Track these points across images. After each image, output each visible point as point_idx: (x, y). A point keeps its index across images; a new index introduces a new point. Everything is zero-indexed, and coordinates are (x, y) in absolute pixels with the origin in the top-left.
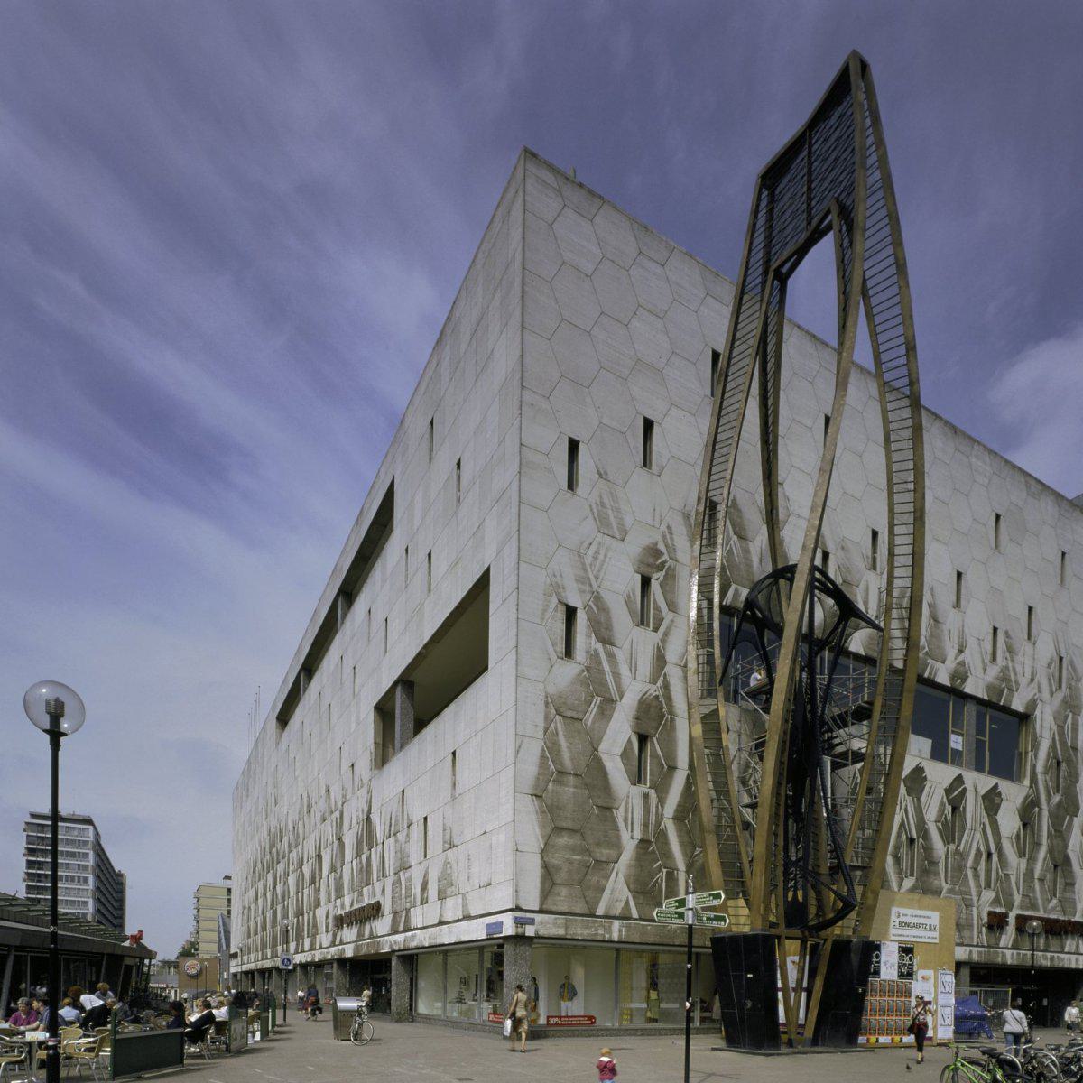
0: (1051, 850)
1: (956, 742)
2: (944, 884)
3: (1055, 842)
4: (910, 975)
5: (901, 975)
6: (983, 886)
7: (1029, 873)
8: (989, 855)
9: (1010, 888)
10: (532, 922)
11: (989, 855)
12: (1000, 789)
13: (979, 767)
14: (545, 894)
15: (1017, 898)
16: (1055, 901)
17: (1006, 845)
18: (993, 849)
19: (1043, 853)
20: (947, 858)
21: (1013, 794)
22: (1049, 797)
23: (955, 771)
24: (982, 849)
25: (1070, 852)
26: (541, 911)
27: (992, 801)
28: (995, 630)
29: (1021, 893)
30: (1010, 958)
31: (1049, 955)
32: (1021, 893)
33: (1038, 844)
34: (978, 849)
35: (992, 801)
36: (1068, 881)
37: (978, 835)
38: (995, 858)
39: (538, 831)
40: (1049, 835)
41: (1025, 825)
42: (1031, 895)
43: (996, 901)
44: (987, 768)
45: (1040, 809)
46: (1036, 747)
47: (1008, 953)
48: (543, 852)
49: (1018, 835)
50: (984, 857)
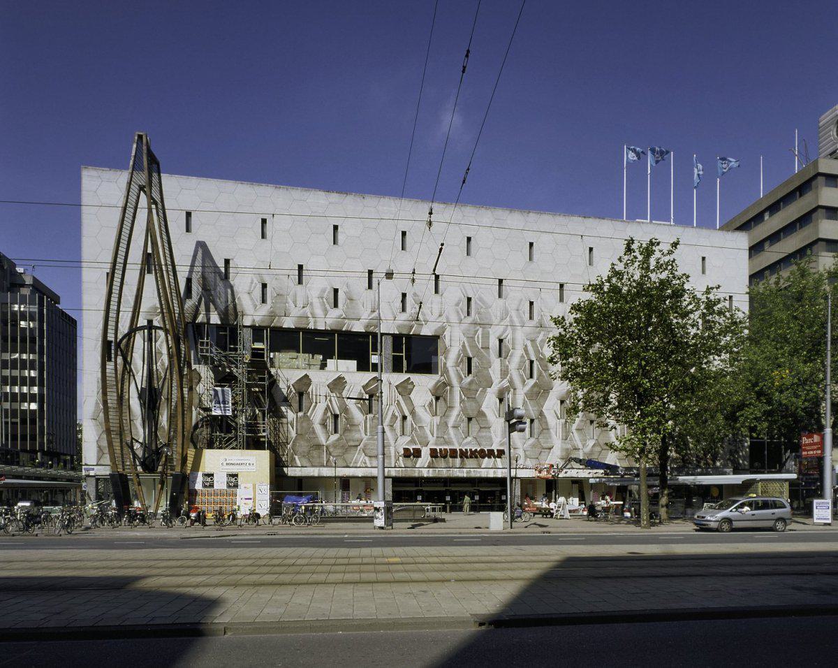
0: (463, 410)
1: (374, 359)
2: (363, 435)
3: (467, 404)
4: (236, 486)
5: (229, 486)
6: (399, 434)
7: (443, 425)
8: (404, 418)
9: (424, 433)
10: (93, 469)
11: (404, 418)
12: (412, 380)
13: (397, 368)
14: (99, 459)
15: (432, 440)
16: (469, 439)
17: (420, 411)
18: (407, 413)
19: (455, 412)
20: (366, 422)
21: (423, 384)
22: (461, 379)
23: (375, 374)
24: (397, 414)
25: (484, 408)
26: (97, 465)
27: (405, 388)
28: (404, 295)
29: (435, 435)
30: (426, 473)
31: (465, 470)
32: (435, 435)
33: (451, 408)
34: (393, 415)
35: (405, 389)
36: (482, 426)
37: (393, 408)
38: (409, 418)
39: (95, 433)
40: (462, 401)
41: (437, 399)
42: (445, 437)
43: (413, 441)
44: (405, 369)
45: (452, 387)
46: (446, 351)
47: (423, 468)
48: (97, 442)
49: (431, 404)
50: (399, 418)
